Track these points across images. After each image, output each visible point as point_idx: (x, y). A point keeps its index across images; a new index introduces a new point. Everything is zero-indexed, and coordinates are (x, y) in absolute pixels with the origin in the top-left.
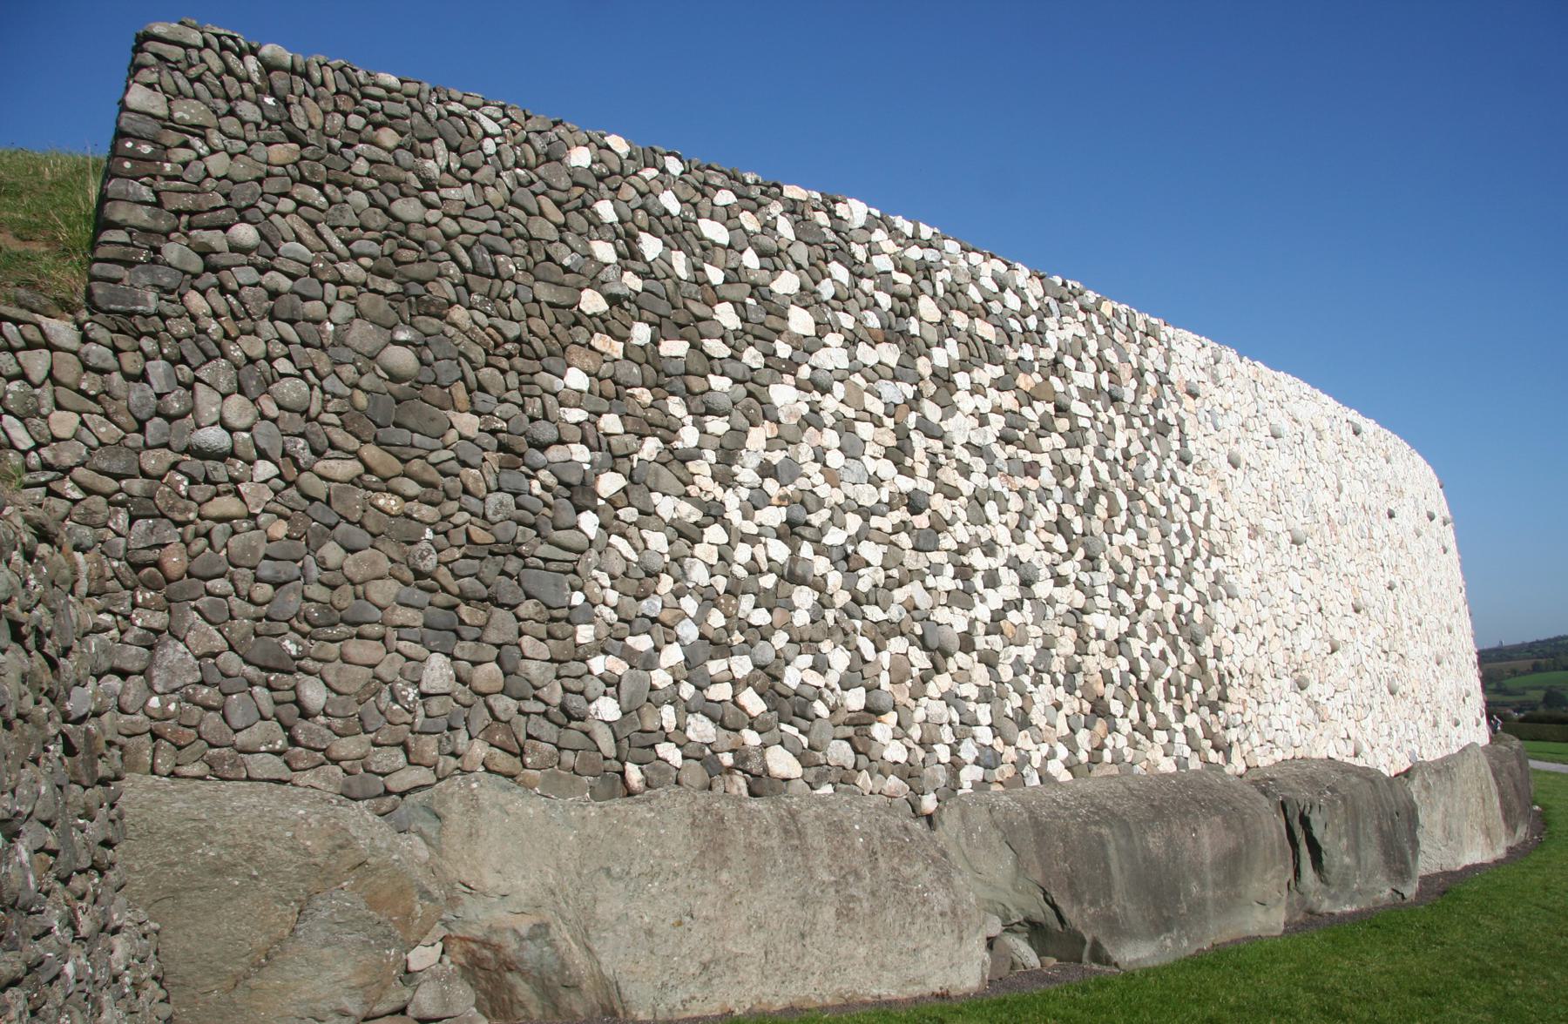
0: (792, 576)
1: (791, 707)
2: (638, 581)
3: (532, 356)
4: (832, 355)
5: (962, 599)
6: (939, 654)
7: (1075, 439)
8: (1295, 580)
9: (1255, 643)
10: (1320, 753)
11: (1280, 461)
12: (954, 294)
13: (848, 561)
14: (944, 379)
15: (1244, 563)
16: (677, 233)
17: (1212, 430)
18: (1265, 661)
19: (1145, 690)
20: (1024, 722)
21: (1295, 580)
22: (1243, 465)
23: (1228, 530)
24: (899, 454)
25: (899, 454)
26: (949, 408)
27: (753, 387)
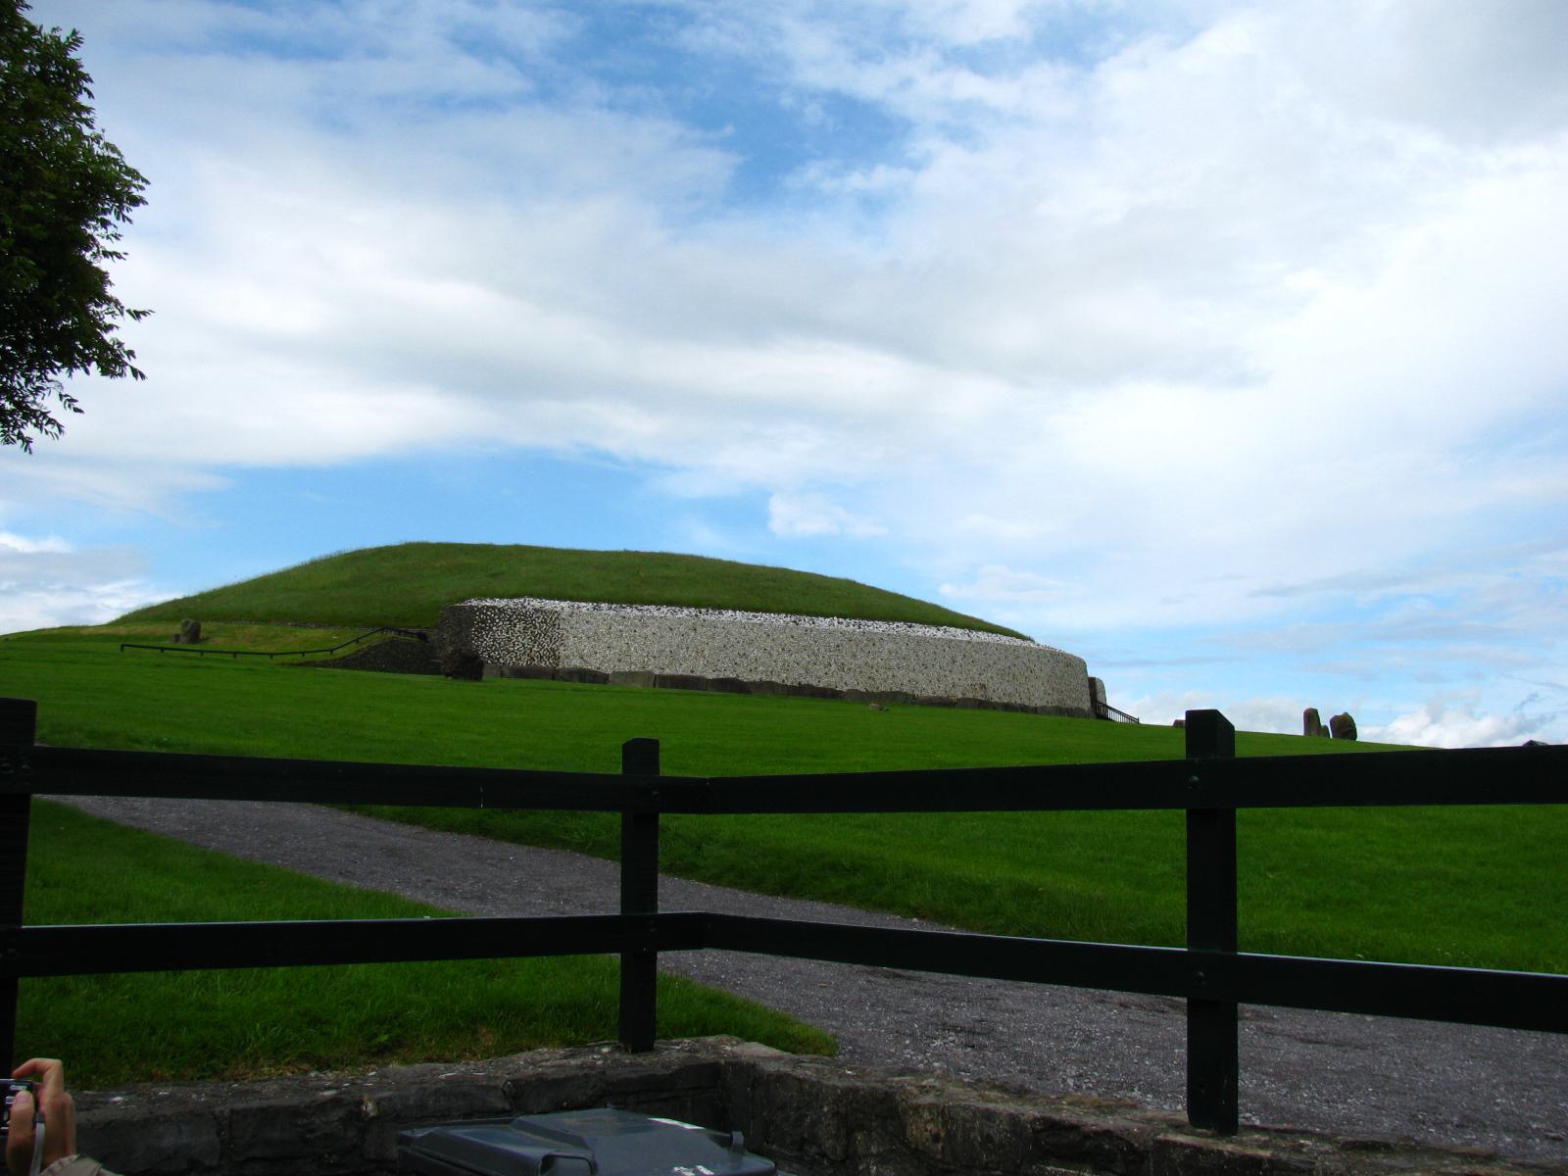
0: (493, 645)
1: (492, 657)
2: (478, 646)
3: (468, 628)
4: (501, 623)
5: (514, 647)
6: (509, 653)
7: (535, 628)
12: (519, 614)
13: (499, 644)
14: (515, 625)
16: (485, 614)
19: (542, 657)
20: (520, 659)
23: (567, 637)
24: (507, 633)
25: (507, 633)
26: (515, 627)
27: (491, 628)
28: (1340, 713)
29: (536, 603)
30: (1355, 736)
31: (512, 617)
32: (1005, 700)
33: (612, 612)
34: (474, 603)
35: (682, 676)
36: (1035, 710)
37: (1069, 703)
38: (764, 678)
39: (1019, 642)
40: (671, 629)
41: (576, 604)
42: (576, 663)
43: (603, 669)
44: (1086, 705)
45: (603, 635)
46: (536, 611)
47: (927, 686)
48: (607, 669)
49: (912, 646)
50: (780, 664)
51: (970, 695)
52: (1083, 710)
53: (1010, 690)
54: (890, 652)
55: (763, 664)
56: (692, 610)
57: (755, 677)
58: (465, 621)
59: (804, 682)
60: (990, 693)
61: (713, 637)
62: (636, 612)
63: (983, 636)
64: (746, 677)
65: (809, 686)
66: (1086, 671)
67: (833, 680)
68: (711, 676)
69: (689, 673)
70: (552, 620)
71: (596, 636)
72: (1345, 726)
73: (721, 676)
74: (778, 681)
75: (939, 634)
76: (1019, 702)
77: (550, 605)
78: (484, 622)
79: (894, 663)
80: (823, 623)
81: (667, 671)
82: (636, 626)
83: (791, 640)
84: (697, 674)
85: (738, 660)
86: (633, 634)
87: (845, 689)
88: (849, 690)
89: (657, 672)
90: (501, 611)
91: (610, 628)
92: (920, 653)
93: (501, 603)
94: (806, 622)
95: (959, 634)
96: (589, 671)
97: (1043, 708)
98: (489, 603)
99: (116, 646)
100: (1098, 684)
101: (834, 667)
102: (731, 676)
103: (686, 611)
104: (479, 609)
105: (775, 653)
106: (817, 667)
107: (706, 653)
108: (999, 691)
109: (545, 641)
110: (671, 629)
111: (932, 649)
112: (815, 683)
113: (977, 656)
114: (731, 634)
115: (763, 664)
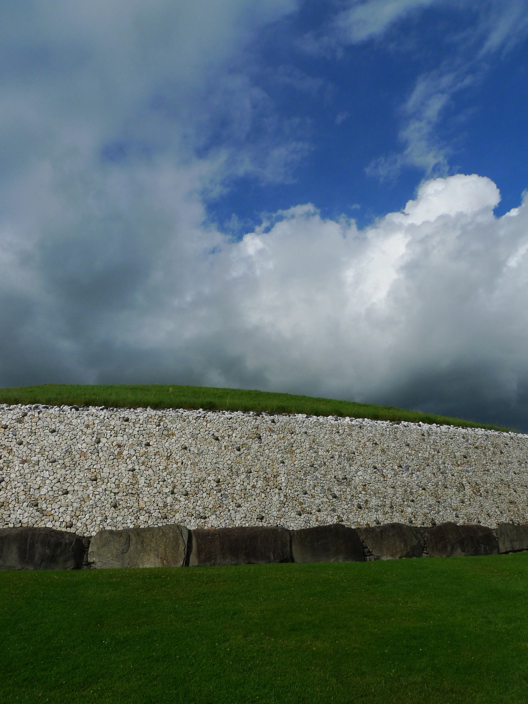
8: (46, 474)
9: (10, 493)
10: (41, 525)
11: (52, 438)
17: (11, 436)
18: (13, 498)
21: (46, 474)
22: (24, 443)
35: (242, 529)
40: (217, 439)
43: (79, 529)
45: (83, 454)
50: (400, 491)
55: (376, 493)
61: (290, 450)
64: (356, 520)
65: (449, 528)
67: (471, 510)
68: (295, 523)
73: (314, 524)
74: (402, 521)
81: (214, 522)
82: (151, 435)
83: (407, 449)
84: (269, 522)
85: (336, 490)
86: (143, 450)
89: (192, 525)
91: (99, 442)
96: (50, 532)
101: (468, 491)
102: (331, 520)
106: (449, 492)
107: (282, 479)
110: (217, 439)
114: (319, 444)
115: (376, 493)
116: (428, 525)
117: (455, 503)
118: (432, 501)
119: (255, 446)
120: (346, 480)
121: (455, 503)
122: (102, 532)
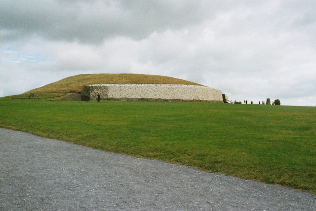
1: (94, 96)
3: (89, 91)
15: (110, 92)
28: (277, 99)
29: (103, 85)
30: (280, 104)
31: (98, 88)
32: (203, 99)
33: (118, 86)
34: (90, 85)
36: (209, 101)
37: (217, 100)
38: (151, 98)
39: (205, 87)
41: (111, 84)
42: (111, 96)
43: (117, 98)
44: (222, 100)
46: (103, 86)
47: (185, 97)
48: (118, 97)
49: (182, 89)
51: (195, 99)
52: (220, 101)
53: (203, 97)
54: (177, 91)
56: (135, 84)
57: (149, 97)
58: (87, 89)
59: (159, 98)
60: (199, 98)
62: (124, 85)
63: (197, 86)
64: (147, 97)
66: (221, 93)
69: (135, 97)
70: (106, 88)
71: (116, 91)
72: (277, 102)
73: (142, 97)
75: (188, 86)
76: (206, 100)
77: (105, 85)
78: (92, 89)
79: (178, 93)
80: (163, 85)
81: (130, 97)
84: (137, 97)
85: (145, 94)
87: (168, 99)
88: (169, 99)
89: (128, 97)
90: (96, 87)
92: (184, 91)
93: (96, 85)
94: (159, 85)
95: (192, 86)
97: (211, 101)
98: (93, 85)
99: (11, 99)
100: (225, 95)
101: (165, 94)
102: (144, 97)
103: (134, 84)
104: (91, 87)
105: (153, 92)
108: (201, 98)
109: (105, 92)
111: (186, 90)
112: (161, 98)
113: (196, 91)
116: (157, 98)
117: (163, 96)
118: (159, 96)
119: (135, 89)
120: (146, 93)
121: (163, 96)
122: (119, 98)
